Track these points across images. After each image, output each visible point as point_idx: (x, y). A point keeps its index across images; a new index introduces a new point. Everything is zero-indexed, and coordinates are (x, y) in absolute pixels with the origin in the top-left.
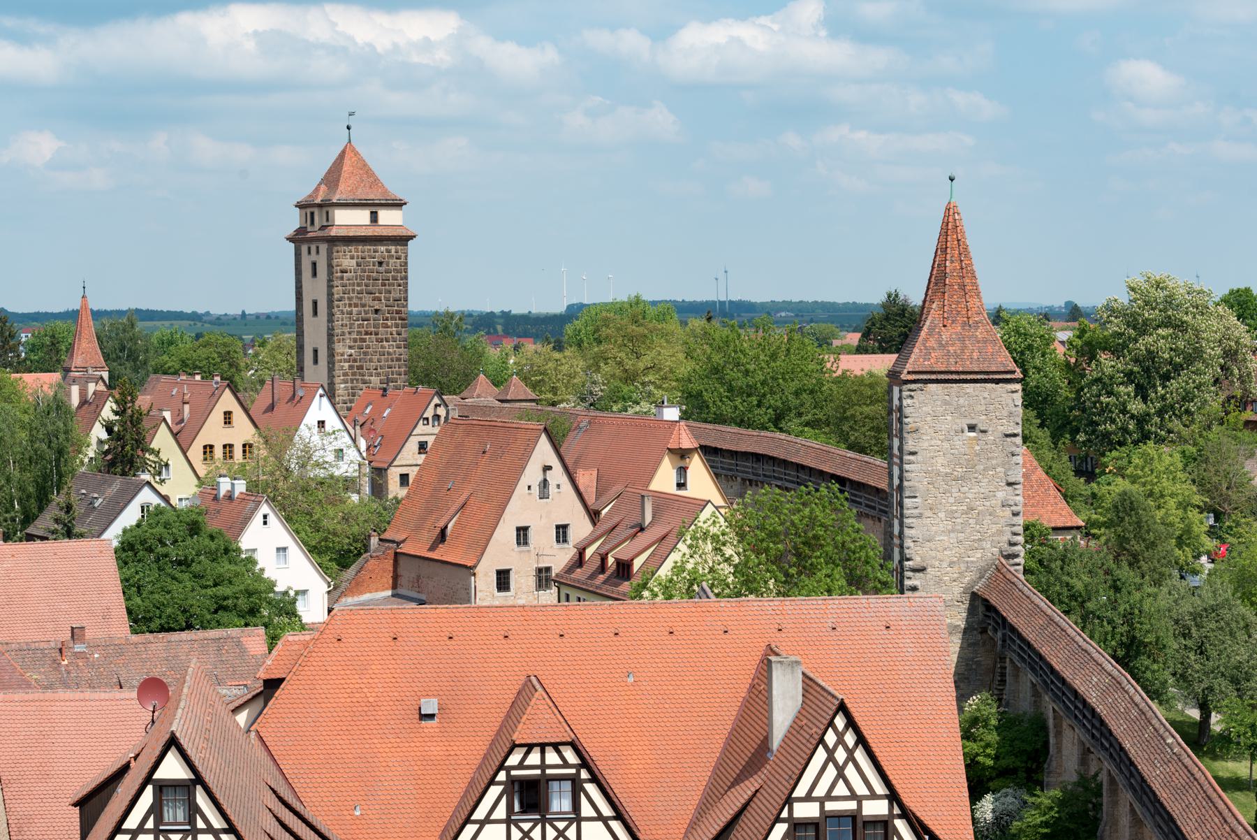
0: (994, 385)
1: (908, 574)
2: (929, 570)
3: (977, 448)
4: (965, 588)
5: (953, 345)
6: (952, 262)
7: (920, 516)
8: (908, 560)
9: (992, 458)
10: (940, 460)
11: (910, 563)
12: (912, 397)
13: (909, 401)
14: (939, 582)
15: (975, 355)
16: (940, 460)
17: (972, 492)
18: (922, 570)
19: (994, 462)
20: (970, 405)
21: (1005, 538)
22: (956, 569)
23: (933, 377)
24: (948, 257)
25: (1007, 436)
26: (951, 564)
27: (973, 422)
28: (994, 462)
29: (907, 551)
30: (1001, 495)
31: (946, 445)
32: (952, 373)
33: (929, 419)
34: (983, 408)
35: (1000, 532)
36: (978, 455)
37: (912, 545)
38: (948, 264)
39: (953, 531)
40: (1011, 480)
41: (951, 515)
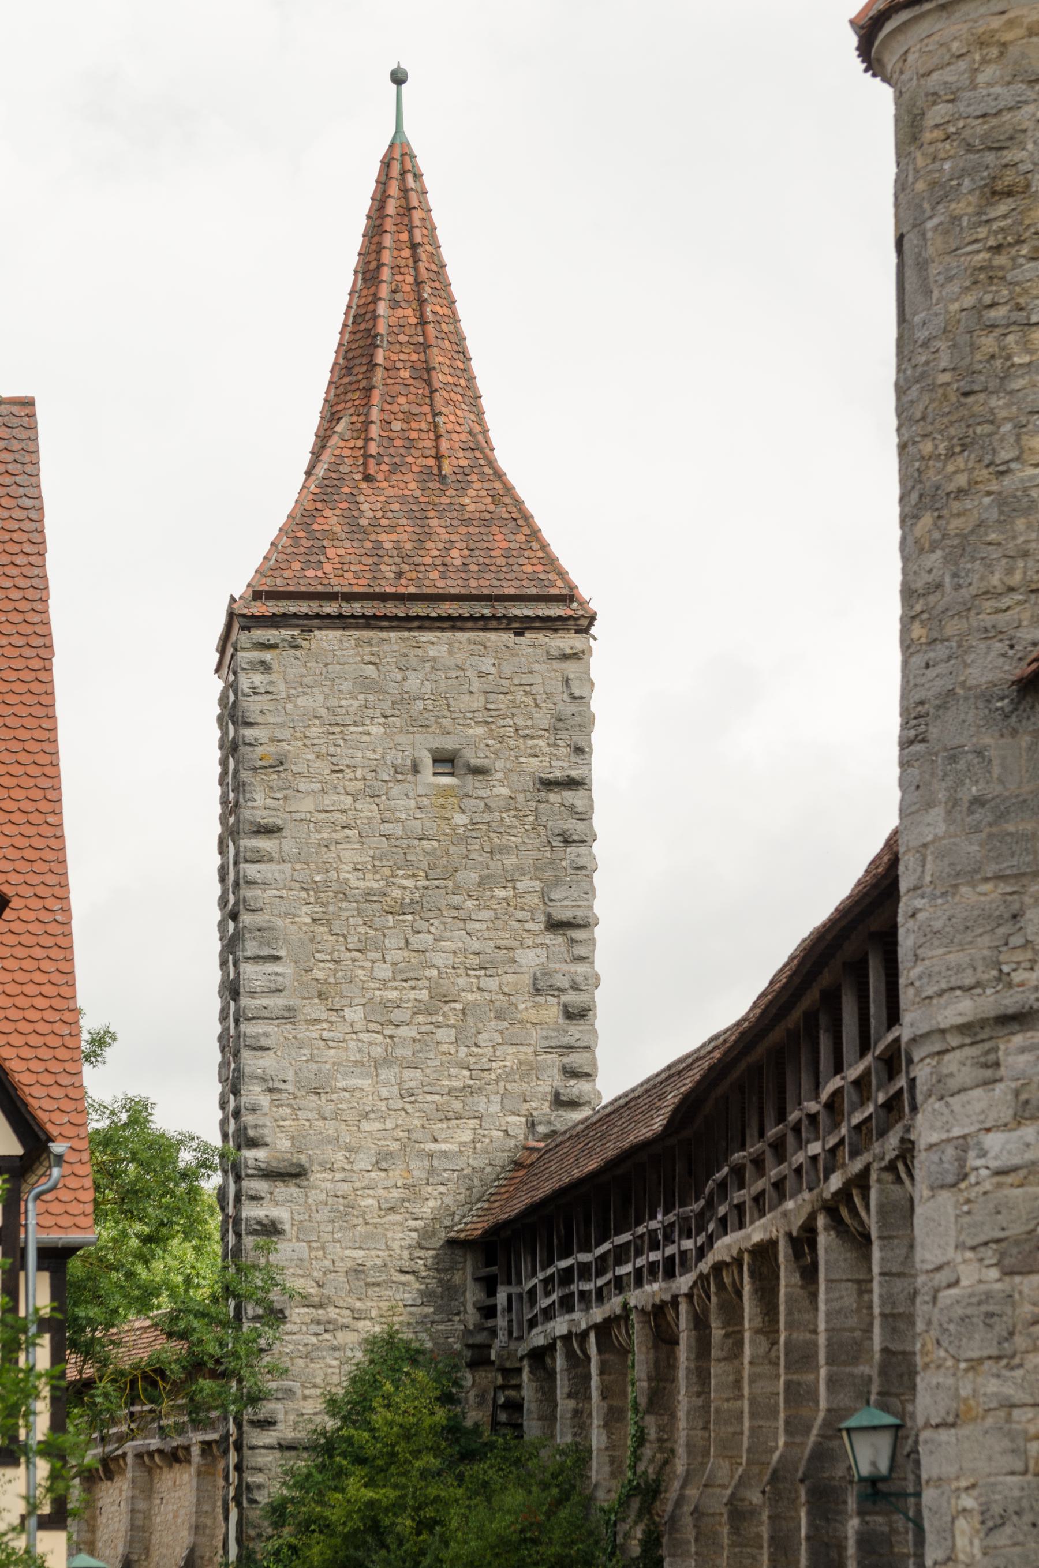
0: (508, 637)
1: (260, 1186)
2: (317, 1176)
3: (460, 819)
4: (426, 1234)
5: (392, 529)
6: (394, 304)
7: (289, 1015)
8: (253, 1143)
9: (505, 850)
10: (350, 854)
11: (261, 1154)
12: (265, 667)
13: (258, 679)
14: (346, 1211)
15: (456, 557)
16: (350, 854)
17: (446, 947)
18: (292, 1174)
19: (511, 861)
20: (436, 695)
21: (545, 1088)
22: (397, 1175)
23: (330, 608)
24: (384, 291)
25: (548, 784)
26: (382, 1161)
27: (449, 743)
28: (511, 861)
29: (248, 1119)
30: (530, 959)
31: (367, 809)
32: (384, 597)
33: (315, 731)
34: (478, 702)
35: (529, 1069)
36: (464, 840)
37: (264, 1100)
38: (382, 308)
39: (387, 1061)
40: (561, 914)
41: (382, 1015)
